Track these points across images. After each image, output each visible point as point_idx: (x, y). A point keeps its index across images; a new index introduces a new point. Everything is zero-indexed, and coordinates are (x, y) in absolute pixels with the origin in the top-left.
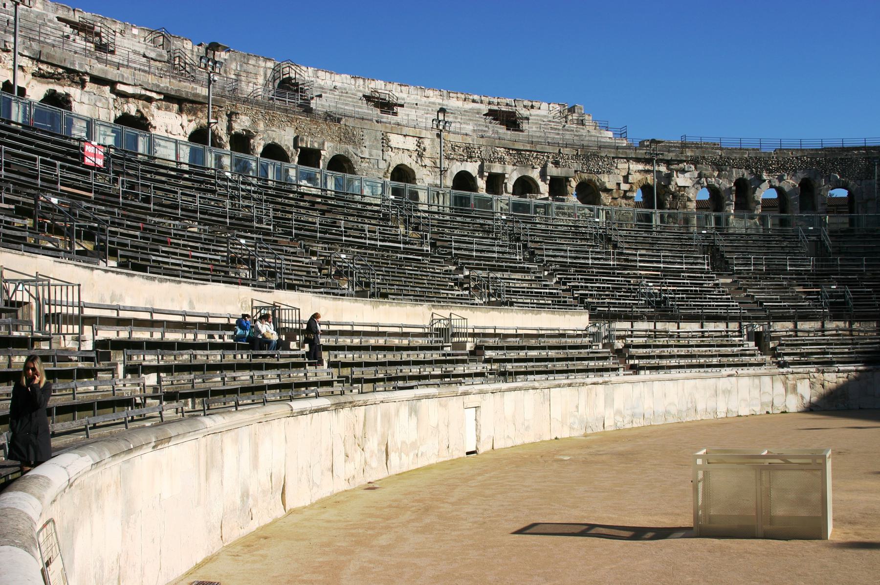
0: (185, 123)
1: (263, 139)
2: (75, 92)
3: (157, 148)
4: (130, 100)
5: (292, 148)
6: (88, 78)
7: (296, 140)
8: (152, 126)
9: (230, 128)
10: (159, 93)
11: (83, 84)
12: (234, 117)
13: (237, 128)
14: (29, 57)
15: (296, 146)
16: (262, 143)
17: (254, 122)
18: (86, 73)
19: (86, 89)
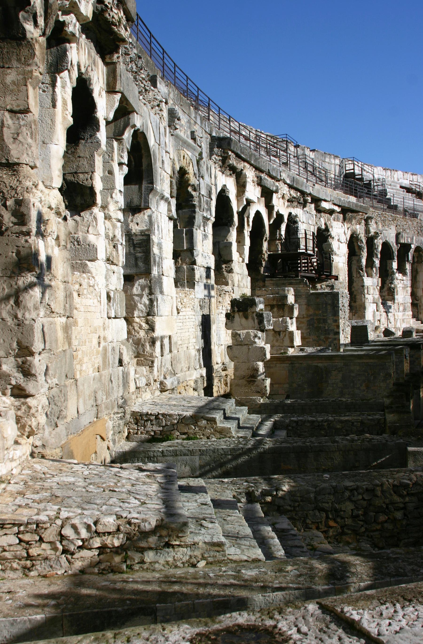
0: (346, 232)
1: (381, 239)
2: (297, 211)
3: (334, 257)
4: (322, 214)
5: (395, 244)
6: (309, 199)
7: (398, 235)
8: (331, 237)
9: (367, 231)
10: (339, 206)
11: (304, 205)
12: (369, 221)
13: (372, 231)
14: (288, 185)
15: (397, 242)
16: (381, 242)
17: (376, 223)
18: (310, 194)
19: (305, 209)
